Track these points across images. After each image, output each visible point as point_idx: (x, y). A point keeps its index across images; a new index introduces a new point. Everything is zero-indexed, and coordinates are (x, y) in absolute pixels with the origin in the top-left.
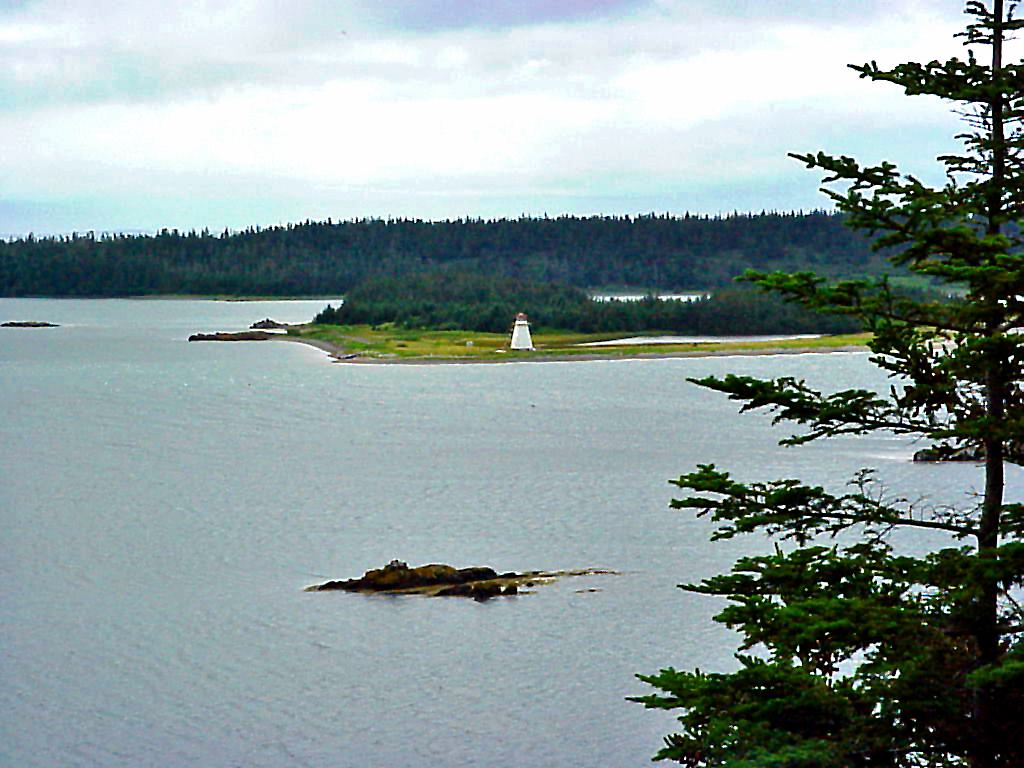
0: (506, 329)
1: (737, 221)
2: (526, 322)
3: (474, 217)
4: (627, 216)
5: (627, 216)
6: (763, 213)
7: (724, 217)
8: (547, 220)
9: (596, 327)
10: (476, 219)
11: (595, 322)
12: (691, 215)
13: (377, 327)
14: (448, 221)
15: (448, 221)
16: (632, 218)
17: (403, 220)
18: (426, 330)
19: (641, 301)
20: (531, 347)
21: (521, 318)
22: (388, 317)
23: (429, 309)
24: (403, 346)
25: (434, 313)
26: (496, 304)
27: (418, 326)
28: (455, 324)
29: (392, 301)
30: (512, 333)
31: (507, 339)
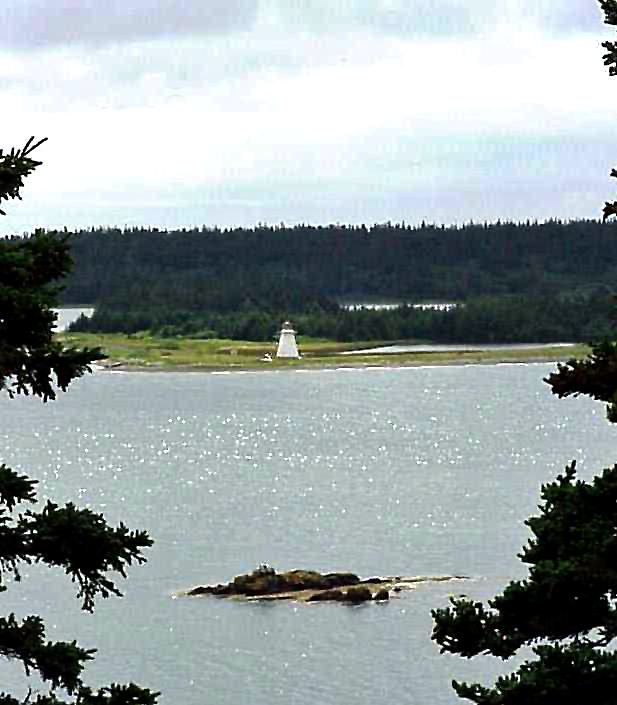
0: (272, 336)
1: (472, 231)
2: (292, 331)
3: (211, 227)
4: (363, 226)
5: (363, 226)
6: (499, 223)
7: (460, 226)
8: (283, 229)
9: (352, 335)
10: (212, 228)
11: (352, 330)
12: (426, 224)
13: (134, 335)
14: (184, 230)
15: (184, 230)
16: (368, 227)
17: (140, 229)
18: (183, 339)
19: (396, 309)
20: (297, 355)
21: (288, 327)
22: (142, 326)
23: (184, 318)
24: (168, 354)
25: (191, 322)
26: (254, 313)
27: (174, 334)
28: (212, 332)
29: (146, 310)
30: (278, 341)
31: (274, 347)
